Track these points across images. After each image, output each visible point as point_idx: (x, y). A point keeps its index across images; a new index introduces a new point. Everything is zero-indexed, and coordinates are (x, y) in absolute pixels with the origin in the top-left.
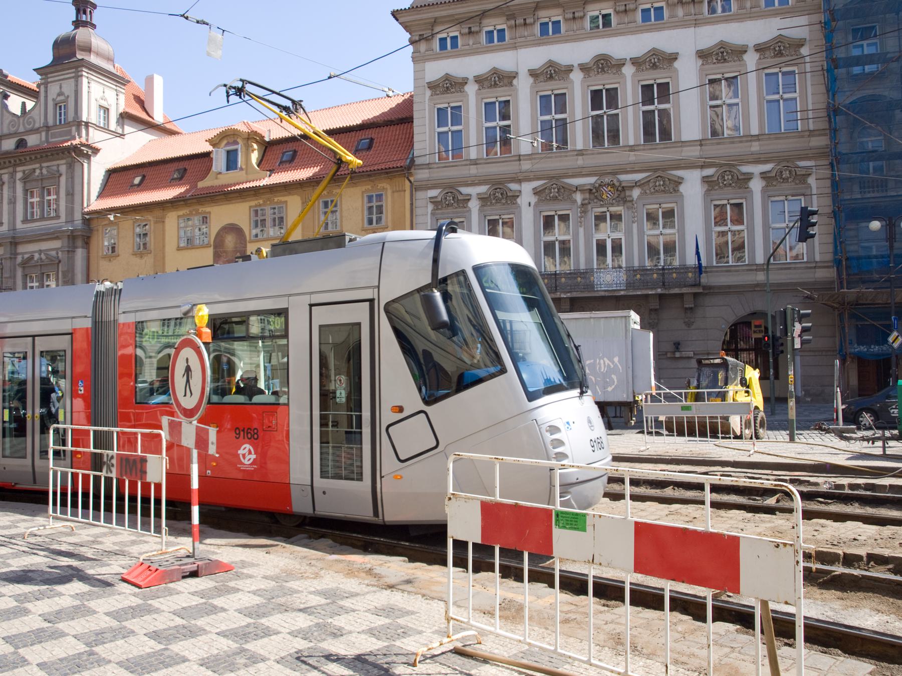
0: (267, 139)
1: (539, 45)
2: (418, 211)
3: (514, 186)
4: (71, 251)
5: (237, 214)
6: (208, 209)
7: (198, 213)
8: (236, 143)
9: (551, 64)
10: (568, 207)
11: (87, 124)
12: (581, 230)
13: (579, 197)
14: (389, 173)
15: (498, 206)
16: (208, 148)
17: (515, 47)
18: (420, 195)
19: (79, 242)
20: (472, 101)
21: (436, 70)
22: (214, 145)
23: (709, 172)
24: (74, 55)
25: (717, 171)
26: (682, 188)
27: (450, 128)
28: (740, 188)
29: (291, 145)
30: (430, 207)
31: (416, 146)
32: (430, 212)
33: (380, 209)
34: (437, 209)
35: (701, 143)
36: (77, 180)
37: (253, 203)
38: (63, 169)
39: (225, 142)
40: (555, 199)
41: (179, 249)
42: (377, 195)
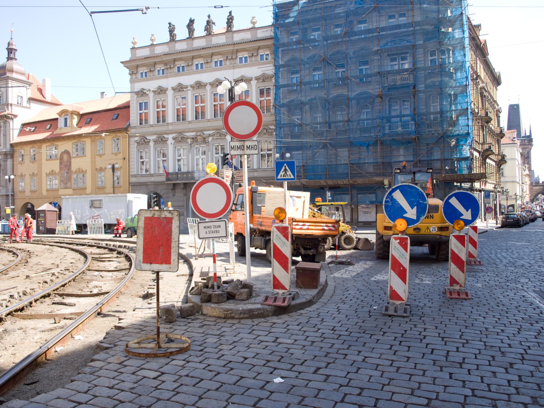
0: (81, 113)
1: (176, 76)
2: (131, 146)
3: (166, 136)
4: (5, 161)
5: (67, 146)
6: (57, 143)
7: (54, 145)
8: (67, 115)
9: (180, 85)
11: (11, 105)
12: (190, 154)
13: (189, 141)
14: (120, 130)
15: (160, 144)
16: (57, 116)
17: (167, 77)
18: (133, 140)
19: (9, 157)
20: (151, 99)
21: (138, 86)
22: (60, 116)
24: (5, 74)
27: (144, 111)
29: (90, 115)
30: (136, 144)
31: (131, 119)
36: (8, 128)
37: (73, 141)
38: (2, 124)
39: (63, 115)
40: (180, 141)
41: (47, 160)
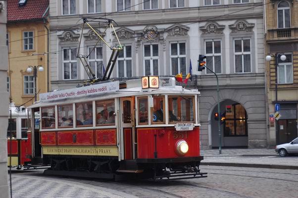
2: (51, 43)
10: (131, 42)
12: (137, 55)
23: (203, 24)
25: (206, 24)
26: (189, 33)
28: (219, 33)
30: (58, 41)
31: (51, 6)
32: (58, 43)
33: (31, 40)
34: (62, 42)
35: (199, 8)
42: (29, 33)
